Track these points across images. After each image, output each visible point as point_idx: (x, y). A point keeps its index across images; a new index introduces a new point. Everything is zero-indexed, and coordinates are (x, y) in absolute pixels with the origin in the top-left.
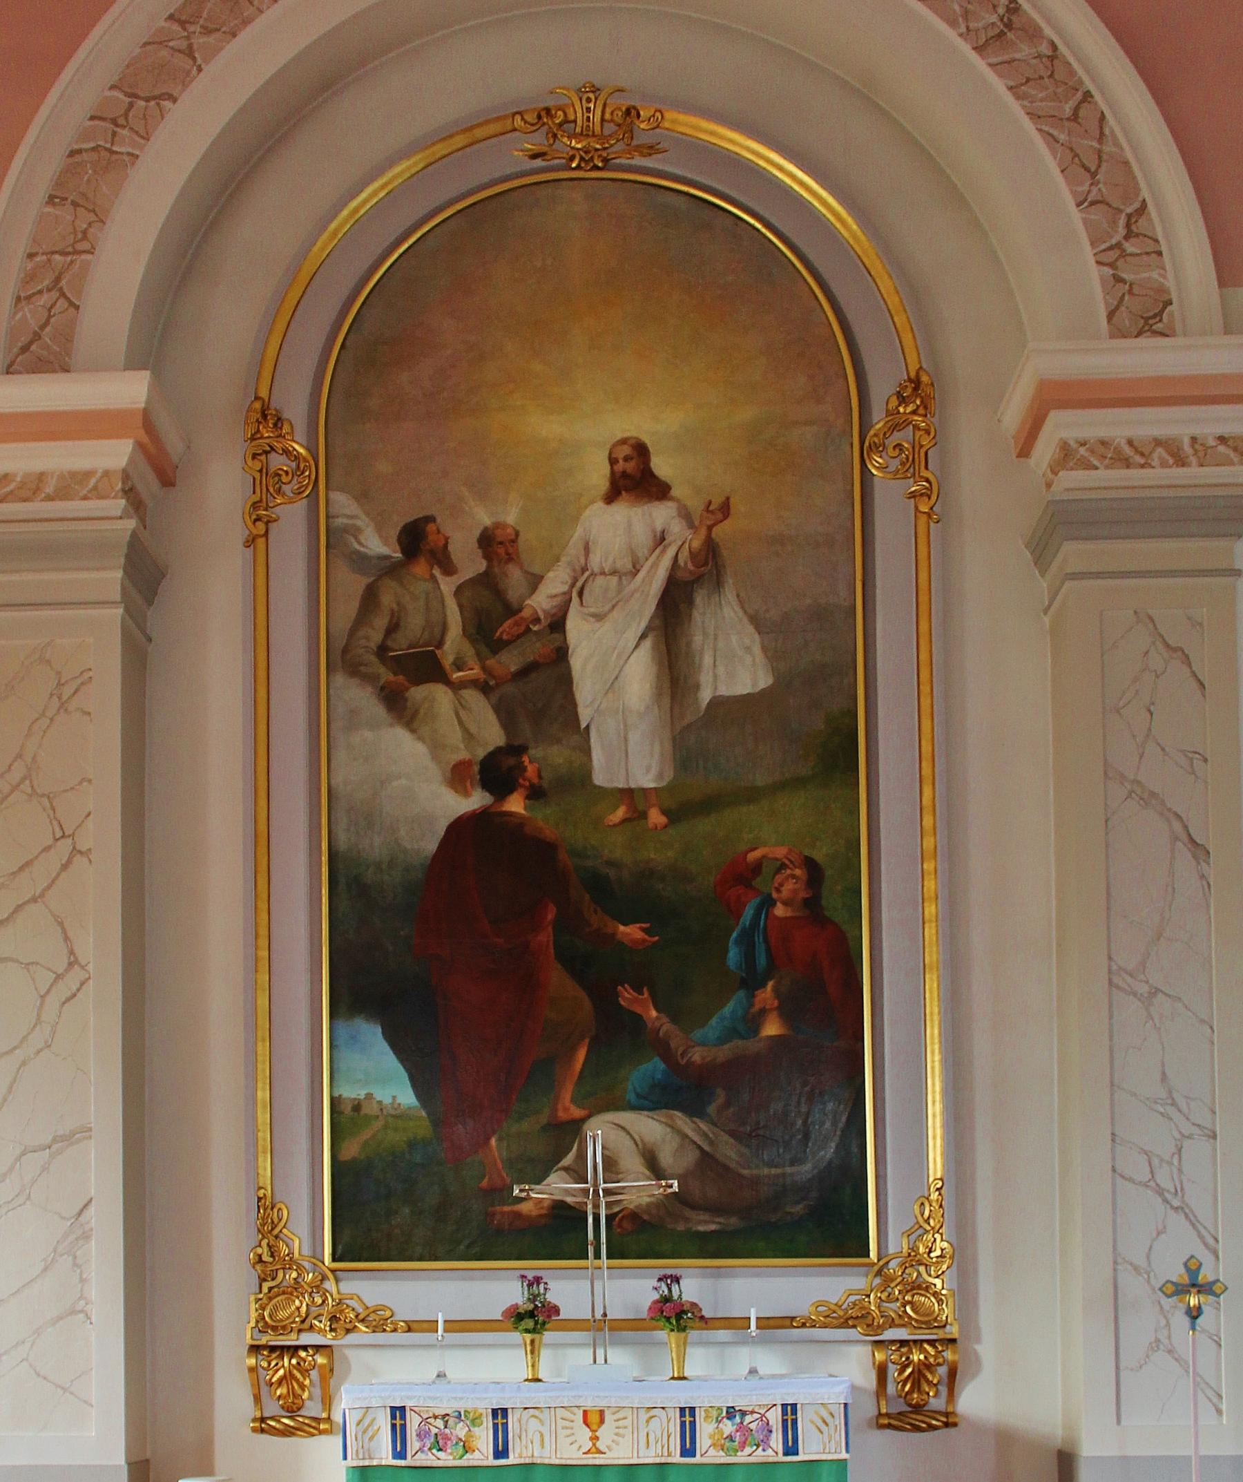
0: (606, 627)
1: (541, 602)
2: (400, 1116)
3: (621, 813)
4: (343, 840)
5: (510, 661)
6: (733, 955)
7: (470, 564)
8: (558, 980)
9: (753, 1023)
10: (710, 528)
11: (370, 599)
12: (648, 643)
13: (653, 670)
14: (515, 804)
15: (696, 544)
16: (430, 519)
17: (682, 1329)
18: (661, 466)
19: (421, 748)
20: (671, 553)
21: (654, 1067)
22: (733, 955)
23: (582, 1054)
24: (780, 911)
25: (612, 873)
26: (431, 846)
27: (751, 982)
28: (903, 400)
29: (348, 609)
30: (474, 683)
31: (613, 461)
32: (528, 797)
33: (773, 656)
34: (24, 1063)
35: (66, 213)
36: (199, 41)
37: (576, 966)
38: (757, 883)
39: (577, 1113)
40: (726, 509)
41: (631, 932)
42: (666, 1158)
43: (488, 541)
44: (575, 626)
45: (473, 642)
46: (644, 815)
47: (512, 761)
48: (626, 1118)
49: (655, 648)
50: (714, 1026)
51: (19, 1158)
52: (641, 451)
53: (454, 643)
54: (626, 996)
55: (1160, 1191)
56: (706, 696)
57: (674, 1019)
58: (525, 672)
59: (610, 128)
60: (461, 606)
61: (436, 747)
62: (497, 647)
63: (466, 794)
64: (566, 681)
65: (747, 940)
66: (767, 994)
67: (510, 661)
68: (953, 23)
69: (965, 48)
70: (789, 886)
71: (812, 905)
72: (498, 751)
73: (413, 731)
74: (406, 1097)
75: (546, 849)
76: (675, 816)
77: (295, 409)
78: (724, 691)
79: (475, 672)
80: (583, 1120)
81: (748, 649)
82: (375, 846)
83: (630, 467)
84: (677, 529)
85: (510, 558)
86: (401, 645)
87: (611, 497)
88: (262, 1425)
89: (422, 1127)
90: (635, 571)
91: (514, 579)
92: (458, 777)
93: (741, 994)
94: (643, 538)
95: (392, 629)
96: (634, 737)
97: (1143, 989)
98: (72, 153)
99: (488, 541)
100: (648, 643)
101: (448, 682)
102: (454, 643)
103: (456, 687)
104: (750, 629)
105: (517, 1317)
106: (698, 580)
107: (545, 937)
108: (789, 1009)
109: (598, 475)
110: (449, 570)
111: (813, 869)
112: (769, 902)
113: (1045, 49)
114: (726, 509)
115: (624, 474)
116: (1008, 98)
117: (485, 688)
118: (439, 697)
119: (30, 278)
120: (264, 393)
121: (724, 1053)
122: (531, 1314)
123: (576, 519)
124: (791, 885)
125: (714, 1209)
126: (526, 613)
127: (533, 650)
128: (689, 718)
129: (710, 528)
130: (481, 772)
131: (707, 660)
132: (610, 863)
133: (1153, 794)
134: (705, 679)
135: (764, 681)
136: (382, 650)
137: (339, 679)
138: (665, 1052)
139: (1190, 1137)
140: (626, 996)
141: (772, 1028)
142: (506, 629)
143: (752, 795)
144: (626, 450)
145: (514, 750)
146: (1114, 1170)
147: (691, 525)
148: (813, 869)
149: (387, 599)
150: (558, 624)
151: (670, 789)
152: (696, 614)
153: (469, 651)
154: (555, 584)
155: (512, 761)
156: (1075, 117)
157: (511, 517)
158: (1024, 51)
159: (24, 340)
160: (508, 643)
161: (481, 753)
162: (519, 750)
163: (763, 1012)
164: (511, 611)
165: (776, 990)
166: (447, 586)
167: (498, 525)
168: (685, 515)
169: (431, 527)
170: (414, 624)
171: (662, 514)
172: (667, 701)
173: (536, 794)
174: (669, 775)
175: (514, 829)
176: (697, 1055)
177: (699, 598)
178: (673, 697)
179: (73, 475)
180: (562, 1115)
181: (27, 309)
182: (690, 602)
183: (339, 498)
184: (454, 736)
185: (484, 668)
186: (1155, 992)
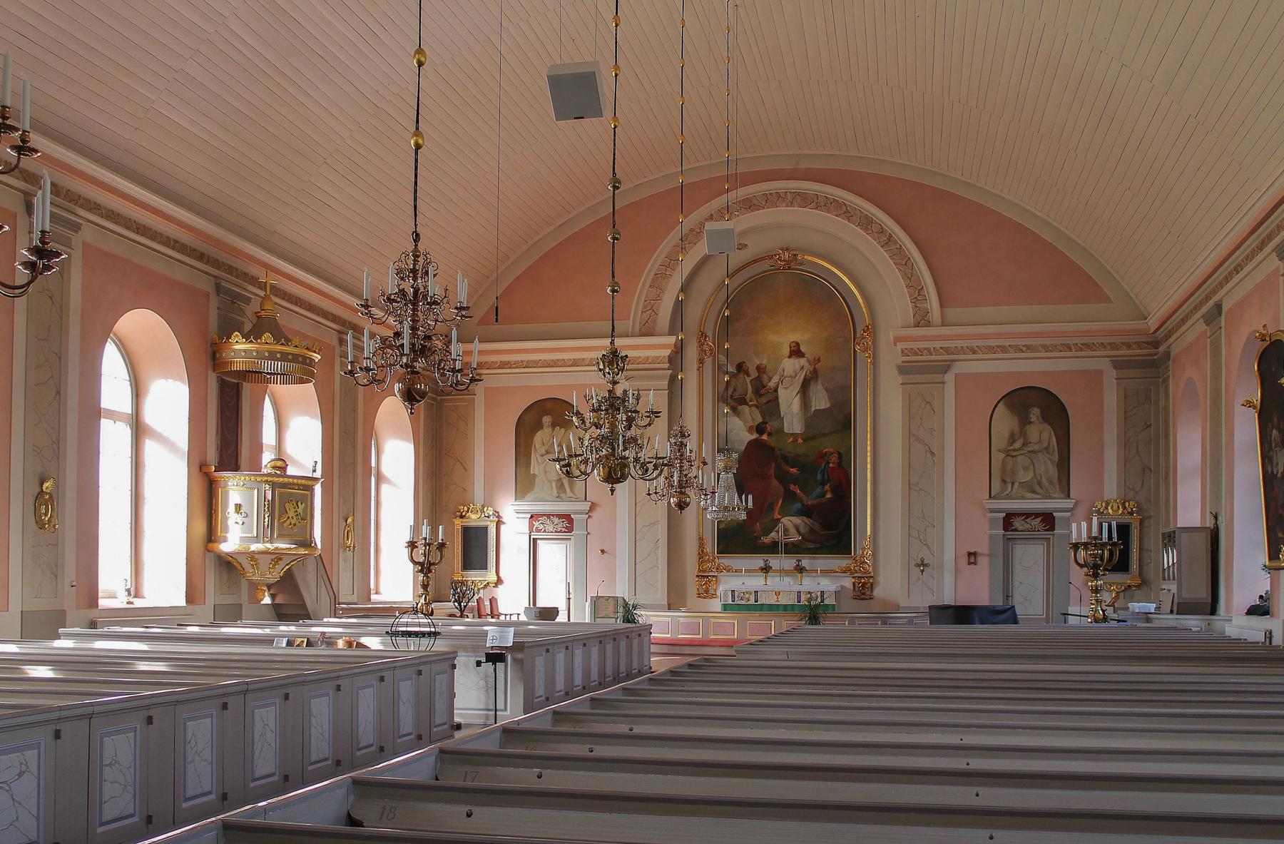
0: (788, 391)
1: (772, 384)
3: (791, 439)
4: (721, 447)
5: (764, 400)
6: (819, 477)
7: (754, 374)
8: (775, 482)
9: (824, 495)
10: (815, 365)
12: (799, 395)
13: (800, 402)
14: (765, 437)
15: (811, 369)
16: (744, 362)
17: (802, 573)
18: (803, 349)
19: (741, 423)
20: (805, 371)
21: (798, 506)
22: (819, 477)
23: (780, 502)
24: (831, 465)
25: (789, 455)
27: (823, 484)
28: (864, 332)
29: (722, 387)
30: (754, 405)
31: (790, 347)
32: (768, 435)
33: (830, 399)
34: (643, 505)
35: (654, 290)
36: (687, 246)
37: (780, 480)
38: (826, 458)
39: (779, 517)
40: (819, 360)
42: (802, 530)
43: (759, 368)
45: (754, 394)
46: (797, 440)
47: (763, 426)
48: (789, 518)
49: (800, 397)
51: (642, 528)
52: (798, 344)
53: (750, 395)
54: (792, 487)
55: (920, 540)
57: (804, 493)
58: (768, 402)
59: (791, 259)
60: (751, 385)
61: (745, 422)
62: (761, 396)
63: (752, 434)
64: (778, 405)
65: (823, 472)
66: (827, 487)
67: (764, 400)
68: (876, 240)
69: (879, 246)
70: (834, 458)
71: (840, 463)
72: (761, 423)
73: (739, 417)
75: (772, 449)
76: (805, 440)
77: (710, 334)
78: (817, 408)
79: (755, 402)
80: (781, 519)
81: (824, 397)
83: (795, 349)
84: (807, 365)
85: (764, 373)
86: (736, 395)
87: (790, 357)
88: (699, 595)
90: (796, 376)
92: (750, 430)
93: (821, 487)
94: (797, 367)
95: (734, 391)
96: (795, 419)
97: (918, 489)
98: (656, 274)
99: (759, 368)
100: (799, 395)
101: (748, 405)
102: (750, 395)
103: (750, 406)
104: (825, 392)
105: (762, 569)
106: (812, 378)
107: (772, 472)
108: (833, 491)
109: (786, 351)
111: (839, 453)
112: (829, 463)
113: (898, 246)
115: (793, 351)
116: (889, 258)
117: (757, 407)
118: (745, 409)
119: (645, 307)
120: (702, 330)
121: (816, 502)
122: (765, 569)
123: (781, 362)
124: (834, 458)
125: (813, 542)
126: (768, 387)
128: (808, 415)
129: (815, 365)
130: (757, 428)
131: (814, 400)
132: (789, 452)
133: (922, 440)
134: (813, 404)
135: (828, 405)
136: (731, 396)
137: (720, 404)
138: (800, 500)
139: (928, 527)
140: (792, 487)
141: (829, 496)
142: (763, 391)
143: (824, 435)
144: (794, 344)
146: (909, 535)
147: (810, 364)
149: (733, 383)
150: (776, 390)
152: (811, 387)
153: (753, 397)
154: (775, 379)
155: (763, 426)
156: (906, 264)
157: (764, 363)
158: (893, 247)
159: (644, 323)
160: (763, 395)
161: (756, 424)
162: (766, 423)
163: (826, 491)
164: (764, 386)
165: (830, 486)
166: (748, 380)
167: (761, 364)
168: (809, 361)
169: (744, 364)
171: (803, 361)
172: (803, 411)
173: (770, 434)
174: (804, 430)
176: (810, 503)
177: (812, 383)
178: (805, 409)
179: (656, 357)
180: (775, 517)
181: (644, 315)
182: (810, 385)
183: (720, 356)
185: (757, 401)
186: (921, 489)
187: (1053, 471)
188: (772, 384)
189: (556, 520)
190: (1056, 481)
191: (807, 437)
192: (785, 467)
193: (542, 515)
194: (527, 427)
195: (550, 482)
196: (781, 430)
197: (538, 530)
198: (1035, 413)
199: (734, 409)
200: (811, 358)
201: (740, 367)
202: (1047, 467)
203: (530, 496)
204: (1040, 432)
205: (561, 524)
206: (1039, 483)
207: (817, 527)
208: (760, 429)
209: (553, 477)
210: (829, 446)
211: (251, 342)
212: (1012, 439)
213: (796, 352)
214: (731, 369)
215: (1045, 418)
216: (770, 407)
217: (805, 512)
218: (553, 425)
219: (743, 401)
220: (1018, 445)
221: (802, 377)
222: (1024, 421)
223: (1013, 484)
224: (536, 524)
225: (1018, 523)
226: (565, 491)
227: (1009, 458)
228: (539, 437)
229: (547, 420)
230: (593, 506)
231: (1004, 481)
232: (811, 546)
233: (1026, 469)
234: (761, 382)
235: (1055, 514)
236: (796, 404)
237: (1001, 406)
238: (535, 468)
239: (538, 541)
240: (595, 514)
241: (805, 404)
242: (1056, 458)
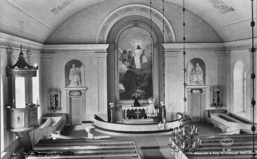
1: (133, 56)
2: (124, 90)
5: (130, 60)
6: (145, 80)
11: (121, 56)
14: (131, 69)
18: (140, 47)
22: (145, 80)
26: (125, 72)
41: (138, 78)
43: (129, 52)
44: (135, 58)
50: (144, 84)
52: (139, 46)
54: (138, 82)
56: (143, 62)
58: (132, 61)
61: (126, 66)
63: (128, 69)
66: (147, 82)
67: (130, 60)
76: (141, 71)
79: (128, 61)
82: (122, 72)
89: (125, 91)
91: (131, 54)
92: (127, 68)
94: (139, 52)
95: (123, 57)
99: (129, 52)
109: (136, 47)
110: (127, 53)
111: (150, 74)
114: (144, 50)
121: (144, 86)
124: (149, 75)
127: (132, 59)
141: (147, 84)
142: (130, 58)
145: (131, 66)
148: (150, 74)
149: (123, 55)
150: (134, 57)
151: (141, 69)
154: (133, 55)
157: (131, 50)
164: (131, 57)
166: (126, 55)
170: (124, 58)
171: (140, 50)
173: (132, 69)
175: (131, 71)
187: (202, 79)
189: (77, 92)
190: (202, 81)
191: (141, 70)
193: (73, 91)
194: (68, 68)
195: (75, 82)
196: (135, 68)
197: (72, 95)
198: (197, 65)
199: (123, 63)
200: (143, 49)
201: (125, 52)
202: (201, 78)
203: (69, 86)
204: (199, 68)
205: (78, 93)
206: (199, 82)
207: (144, 92)
208: (130, 67)
209: (76, 80)
210: (147, 72)
211: (21, 69)
212: (192, 70)
213: (139, 48)
214: (122, 52)
215: (200, 66)
217: (142, 88)
218: (75, 67)
219: (125, 60)
220: (194, 72)
221: (140, 55)
222: (195, 66)
223: (193, 82)
224: (71, 93)
225: (194, 91)
226: (79, 85)
227: (192, 76)
228: (71, 70)
229: (74, 65)
230: (87, 88)
231: (190, 81)
232: (143, 97)
233: (195, 78)
234: (130, 55)
235: (203, 89)
237: (190, 62)
238: (70, 78)
240: (87, 91)
242: (202, 75)
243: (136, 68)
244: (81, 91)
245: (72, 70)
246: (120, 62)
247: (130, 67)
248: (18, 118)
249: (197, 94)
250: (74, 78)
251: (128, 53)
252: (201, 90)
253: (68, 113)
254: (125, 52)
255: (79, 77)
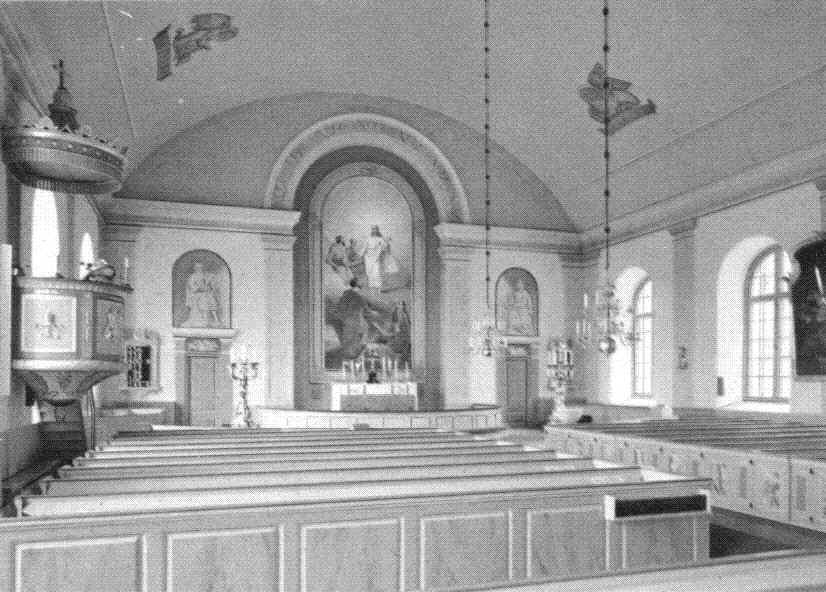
11: (331, 249)
14: (356, 289)
18: (382, 232)
44: (366, 257)
52: (377, 228)
63: (346, 284)
74: (337, 339)
84: (383, 242)
91: (356, 248)
99: (352, 242)
102: (345, 260)
118: (342, 269)
145: (356, 279)
150: (363, 257)
171: (380, 239)
175: (355, 293)
184: (345, 276)
188: (361, 254)
192: (369, 310)
198: (521, 285)
201: (339, 240)
202: (525, 319)
203: (187, 324)
208: (353, 283)
213: (376, 233)
214: (333, 240)
216: (360, 268)
219: (340, 262)
224: (191, 346)
236: (376, 267)
239: (194, 361)
241: (382, 268)
243: (371, 286)
244: (222, 340)
245: (195, 279)
246: (328, 268)
247: (353, 283)
248: (52, 319)
249: (518, 358)
250: (198, 302)
251: (348, 244)
252: (526, 346)
253: (182, 401)
254: (339, 240)
255: (213, 301)
